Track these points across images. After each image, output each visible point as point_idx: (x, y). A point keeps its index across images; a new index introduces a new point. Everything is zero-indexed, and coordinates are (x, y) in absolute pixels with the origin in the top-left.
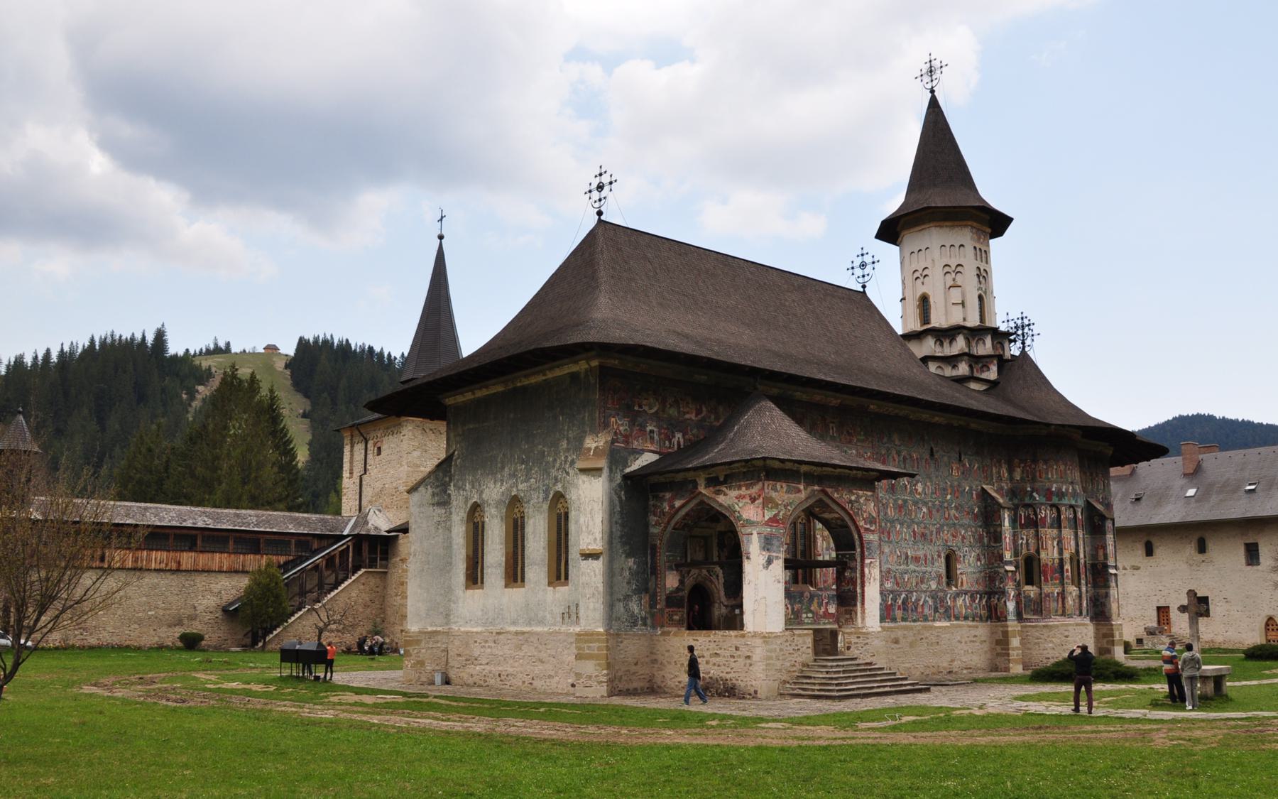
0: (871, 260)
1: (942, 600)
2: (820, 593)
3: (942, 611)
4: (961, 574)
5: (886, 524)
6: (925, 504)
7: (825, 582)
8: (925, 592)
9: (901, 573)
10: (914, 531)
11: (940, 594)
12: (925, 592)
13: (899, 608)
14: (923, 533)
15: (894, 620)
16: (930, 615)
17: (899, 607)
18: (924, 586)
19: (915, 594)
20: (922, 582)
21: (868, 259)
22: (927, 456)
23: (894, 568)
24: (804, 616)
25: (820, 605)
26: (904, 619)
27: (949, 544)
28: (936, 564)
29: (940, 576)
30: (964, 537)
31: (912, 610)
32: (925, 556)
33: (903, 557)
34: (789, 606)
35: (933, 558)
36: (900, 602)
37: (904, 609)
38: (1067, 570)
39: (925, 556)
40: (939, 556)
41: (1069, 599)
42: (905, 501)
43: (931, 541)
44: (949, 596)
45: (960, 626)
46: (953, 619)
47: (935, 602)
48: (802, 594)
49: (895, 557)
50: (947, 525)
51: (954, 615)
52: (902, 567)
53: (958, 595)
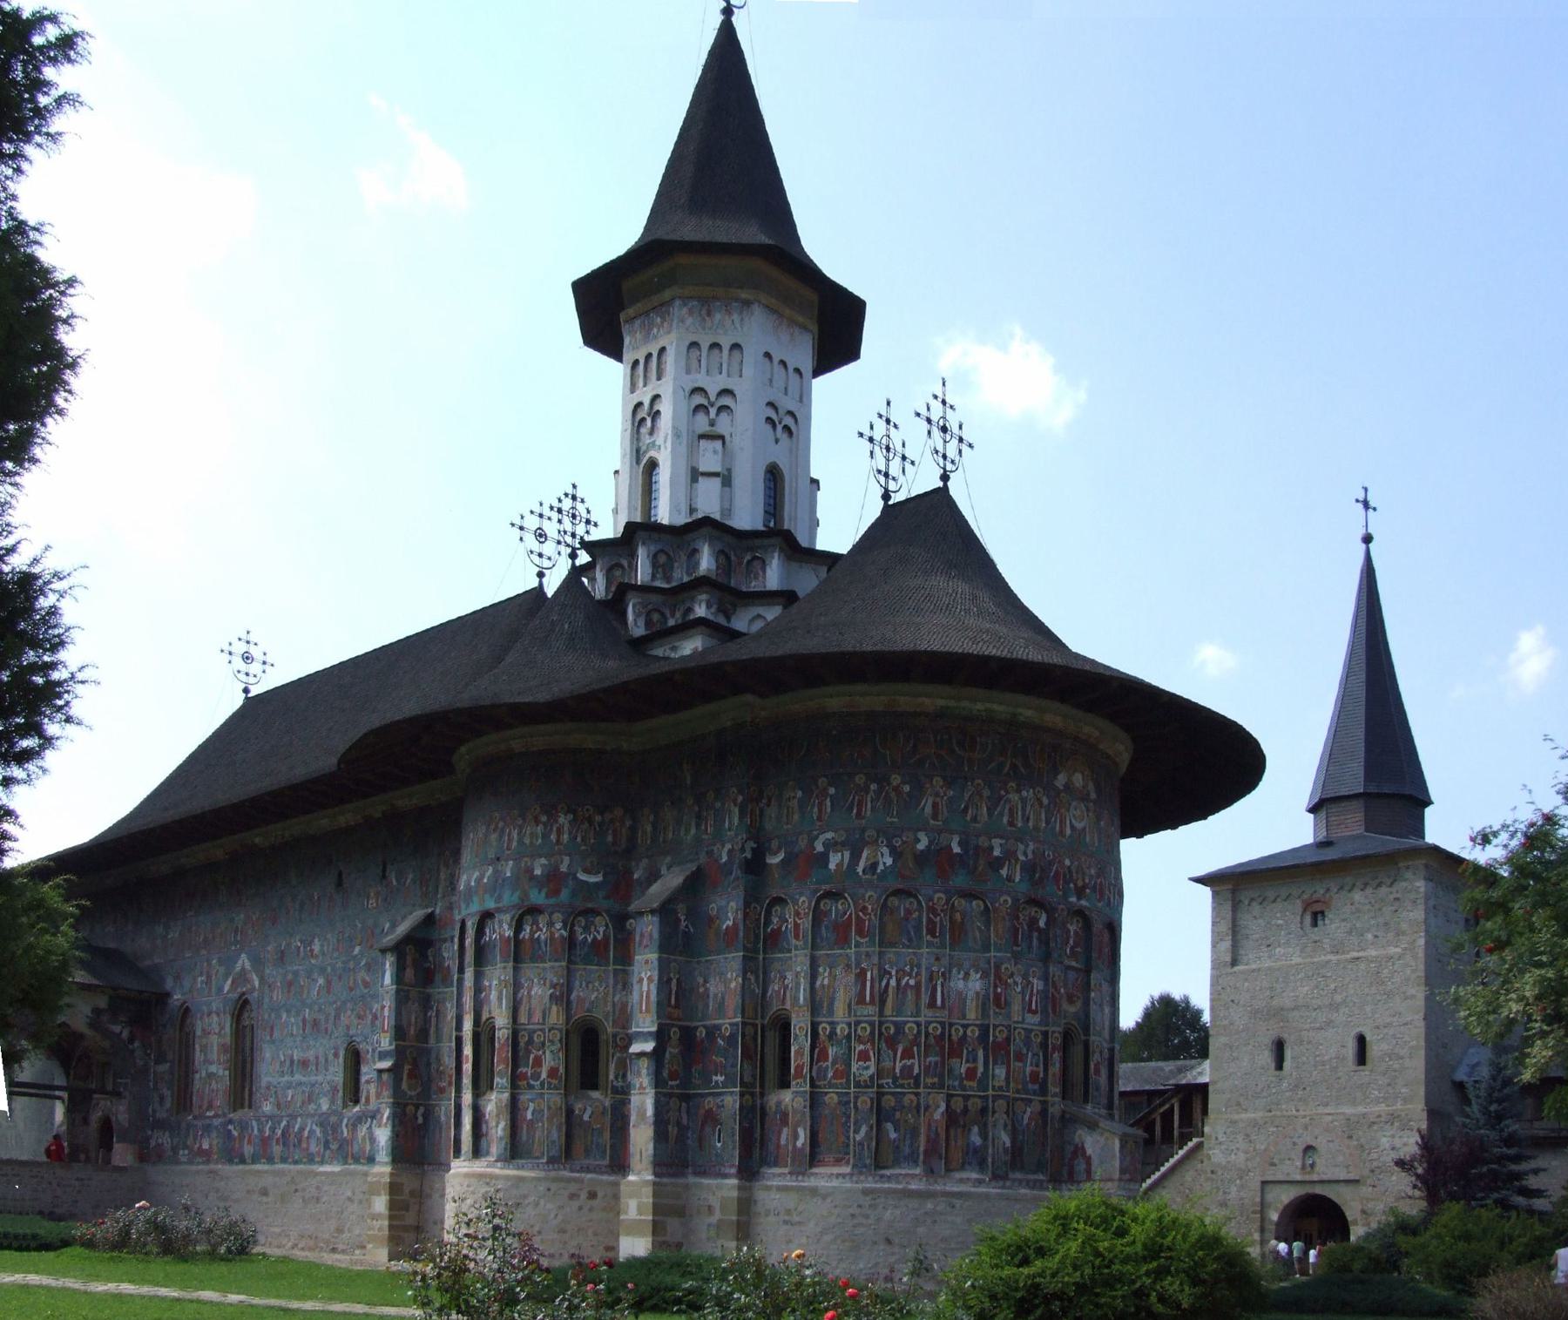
1: (336, 1128)
3: (334, 1146)
4: (368, 1082)
5: (270, 1016)
6: (322, 970)
7: (200, 1107)
8: (313, 1116)
10: (304, 1021)
11: (333, 1119)
12: (313, 1116)
13: (278, 1140)
15: (270, 1160)
16: (318, 1153)
17: (278, 1140)
18: (312, 1107)
19: (299, 1119)
20: (310, 1100)
23: (274, 1081)
24: (181, 1152)
25: (195, 1139)
26: (284, 1160)
27: (351, 1033)
28: (332, 1069)
31: (294, 1146)
32: (317, 1058)
33: (288, 1063)
34: (169, 1140)
35: (326, 1060)
36: (279, 1132)
37: (284, 1144)
39: (317, 1058)
40: (336, 1055)
42: (296, 974)
43: (326, 1033)
44: (345, 1121)
45: (352, 1174)
46: (350, 1161)
47: (325, 1132)
49: (278, 1064)
51: (352, 1154)
52: (286, 1078)
53: (359, 1119)
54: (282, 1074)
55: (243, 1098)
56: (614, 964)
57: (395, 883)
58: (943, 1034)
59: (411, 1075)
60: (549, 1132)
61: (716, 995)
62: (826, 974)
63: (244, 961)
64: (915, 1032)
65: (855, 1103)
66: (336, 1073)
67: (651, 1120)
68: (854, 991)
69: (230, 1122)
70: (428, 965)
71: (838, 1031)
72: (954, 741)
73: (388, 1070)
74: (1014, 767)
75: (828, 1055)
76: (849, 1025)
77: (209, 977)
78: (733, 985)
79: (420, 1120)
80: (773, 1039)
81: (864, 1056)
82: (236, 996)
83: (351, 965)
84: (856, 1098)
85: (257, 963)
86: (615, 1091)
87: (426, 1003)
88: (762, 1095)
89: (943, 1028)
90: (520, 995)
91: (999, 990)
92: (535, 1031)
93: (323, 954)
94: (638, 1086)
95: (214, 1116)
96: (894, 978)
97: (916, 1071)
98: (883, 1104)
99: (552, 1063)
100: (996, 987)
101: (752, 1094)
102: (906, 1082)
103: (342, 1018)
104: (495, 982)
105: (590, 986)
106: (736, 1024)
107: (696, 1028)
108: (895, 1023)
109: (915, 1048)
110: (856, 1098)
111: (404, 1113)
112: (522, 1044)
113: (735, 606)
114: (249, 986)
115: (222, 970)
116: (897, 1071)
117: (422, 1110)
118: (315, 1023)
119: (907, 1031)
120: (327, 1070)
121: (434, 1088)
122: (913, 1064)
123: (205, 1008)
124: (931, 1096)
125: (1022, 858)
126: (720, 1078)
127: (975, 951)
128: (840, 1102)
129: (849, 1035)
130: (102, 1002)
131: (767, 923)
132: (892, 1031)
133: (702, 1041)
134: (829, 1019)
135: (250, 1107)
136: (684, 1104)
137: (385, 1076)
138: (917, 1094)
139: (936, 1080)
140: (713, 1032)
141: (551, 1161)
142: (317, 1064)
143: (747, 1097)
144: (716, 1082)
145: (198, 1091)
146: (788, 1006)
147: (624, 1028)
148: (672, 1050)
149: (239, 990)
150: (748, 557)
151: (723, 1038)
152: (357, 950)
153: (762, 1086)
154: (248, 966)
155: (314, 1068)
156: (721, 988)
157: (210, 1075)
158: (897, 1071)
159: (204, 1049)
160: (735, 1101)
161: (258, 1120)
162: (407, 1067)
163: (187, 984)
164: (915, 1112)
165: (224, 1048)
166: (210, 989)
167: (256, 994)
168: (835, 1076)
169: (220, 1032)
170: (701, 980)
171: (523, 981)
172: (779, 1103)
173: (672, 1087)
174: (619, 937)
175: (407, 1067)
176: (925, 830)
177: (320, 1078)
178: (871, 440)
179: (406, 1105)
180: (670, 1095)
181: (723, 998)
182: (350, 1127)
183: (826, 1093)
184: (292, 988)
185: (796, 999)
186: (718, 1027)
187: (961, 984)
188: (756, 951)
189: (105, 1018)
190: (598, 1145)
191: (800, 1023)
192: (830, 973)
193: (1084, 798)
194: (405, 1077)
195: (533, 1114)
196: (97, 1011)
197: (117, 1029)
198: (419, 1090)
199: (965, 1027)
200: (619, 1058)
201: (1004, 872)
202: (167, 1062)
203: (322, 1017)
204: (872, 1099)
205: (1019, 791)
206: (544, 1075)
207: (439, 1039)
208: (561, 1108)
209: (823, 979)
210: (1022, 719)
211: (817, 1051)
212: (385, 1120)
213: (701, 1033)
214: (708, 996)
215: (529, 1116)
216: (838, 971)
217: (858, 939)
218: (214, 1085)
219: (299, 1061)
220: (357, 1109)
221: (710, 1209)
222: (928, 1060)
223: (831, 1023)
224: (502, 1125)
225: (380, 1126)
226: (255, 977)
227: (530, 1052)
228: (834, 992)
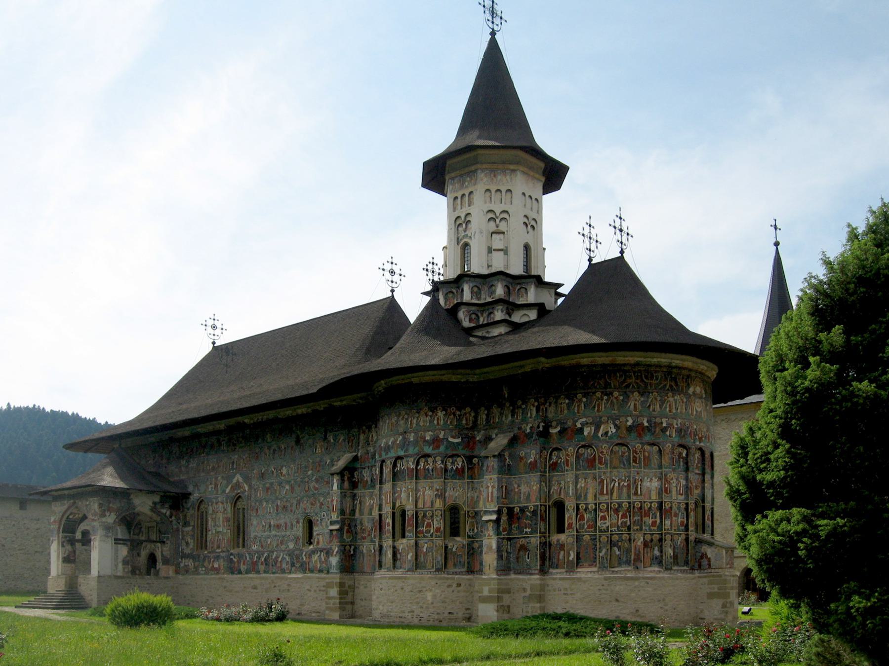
0: (212, 320)
2: (209, 555)
4: (318, 535)
5: (255, 504)
7: (212, 547)
9: (265, 538)
10: (277, 506)
11: (296, 552)
14: (284, 506)
16: (288, 569)
18: (283, 547)
19: (275, 553)
20: (282, 543)
21: (388, 267)
22: (293, 443)
23: (259, 535)
27: (307, 511)
28: (295, 529)
29: (297, 538)
30: (322, 504)
32: (286, 524)
33: (267, 526)
35: (292, 525)
38: (388, 524)
39: (286, 524)
40: (298, 522)
41: (389, 552)
43: (291, 511)
44: (304, 553)
48: (199, 556)
49: (261, 527)
50: (307, 496)
52: (265, 534)
53: (313, 552)
54: (264, 531)
55: (238, 543)
56: (467, 479)
57: (332, 440)
58: (641, 506)
59: (348, 532)
60: (436, 558)
61: (525, 493)
62: (583, 482)
63: (238, 478)
64: (627, 506)
65: (599, 540)
66: (299, 530)
67: (496, 550)
68: (598, 488)
69: (232, 554)
70: (354, 479)
71: (590, 507)
72: (643, 376)
73: (336, 530)
74: (671, 386)
75: (584, 517)
76: (596, 504)
77: (216, 486)
78: (535, 488)
79: (352, 552)
80: (554, 511)
81: (604, 518)
82: (234, 494)
83: (307, 479)
84: (600, 537)
85: (247, 479)
86: (469, 537)
87: (354, 497)
88: (549, 536)
89: (641, 504)
90: (418, 495)
91: (667, 486)
92: (427, 511)
93: (289, 475)
94: (487, 535)
95: (221, 552)
96: (617, 483)
97: (628, 523)
98: (613, 539)
99: (437, 525)
100: (665, 485)
101: (545, 537)
102: (623, 529)
103: (301, 504)
104: (404, 489)
105: (455, 489)
106: (537, 506)
107: (514, 508)
108: (616, 502)
109: (628, 514)
110: (600, 537)
111: (345, 549)
112: (420, 517)
113: (513, 310)
114: (242, 490)
115: (225, 482)
116: (619, 524)
117: (353, 547)
118: (285, 507)
119: (623, 506)
120: (292, 529)
121: (359, 537)
122: (627, 521)
123: (214, 500)
124: (636, 535)
125: (676, 426)
126: (528, 530)
127: (655, 469)
128: (591, 539)
129: (595, 510)
130: (157, 499)
131: (550, 459)
132: (617, 506)
133: (518, 513)
134: (585, 502)
135: (243, 546)
136: (509, 542)
137: (334, 533)
138: (629, 534)
139: (638, 527)
140: (522, 510)
141: (438, 570)
142: (286, 525)
143: (543, 538)
144: (526, 532)
145: (211, 540)
146: (562, 496)
147: (472, 508)
148: (504, 518)
149: (236, 492)
150: (518, 287)
151: (530, 512)
152: (310, 473)
153: (549, 533)
154: (240, 479)
155: (284, 528)
156: (528, 489)
157: (218, 532)
158: (619, 524)
159: (214, 520)
160: (537, 540)
161: (249, 554)
162: (346, 528)
163: (202, 488)
164: (628, 542)
165: (228, 520)
166: (217, 491)
167: (246, 494)
168: (589, 527)
169: (224, 511)
170: (516, 486)
171: (420, 488)
172: (558, 541)
173: (504, 535)
174: (470, 466)
175: (346, 528)
176: (630, 416)
177: (288, 533)
178: (583, 235)
179: (346, 546)
180: (503, 539)
181: (529, 494)
182: (307, 556)
183: (584, 535)
184: (269, 491)
185: (568, 493)
186: (527, 507)
187: (648, 484)
188: (545, 472)
189: (158, 506)
190: (460, 562)
191: (570, 504)
192: (585, 482)
193: (701, 398)
194: (345, 532)
195: (426, 549)
196: (155, 503)
197: (164, 511)
198: (352, 538)
199: (651, 503)
200: (471, 522)
201: (668, 433)
202: (189, 526)
203: (288, 504)
204: (608, 537)
205: (673, 397)
206: (432, 531)
207: (361, 513)
208: (442, 546)
209: (582, 483)
210: (674, 364)
211: (578, 516)
212: (335, 553)
213: (517, 510)
214: (520, 493)
215: (425, 550)
216: (590, 480)
217: (599, 465)
218: (221, 537)
219: (274, 525)
220: (311, 547)
221: (525, 590)
222: (635, 518)
223: (585, 504)
224: (411, 554)
225: (332, 556)
226: (245, 485)
227: (425, 521)
228: (587, 489)
